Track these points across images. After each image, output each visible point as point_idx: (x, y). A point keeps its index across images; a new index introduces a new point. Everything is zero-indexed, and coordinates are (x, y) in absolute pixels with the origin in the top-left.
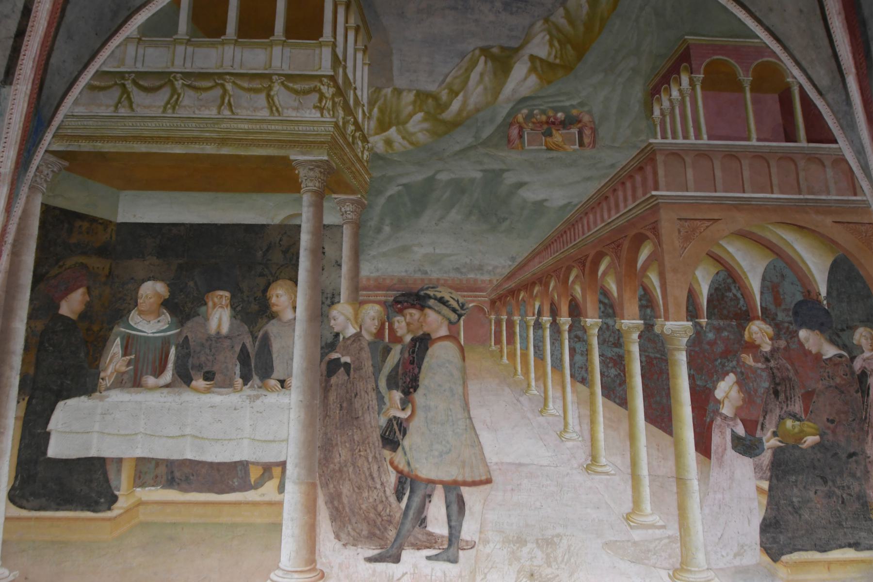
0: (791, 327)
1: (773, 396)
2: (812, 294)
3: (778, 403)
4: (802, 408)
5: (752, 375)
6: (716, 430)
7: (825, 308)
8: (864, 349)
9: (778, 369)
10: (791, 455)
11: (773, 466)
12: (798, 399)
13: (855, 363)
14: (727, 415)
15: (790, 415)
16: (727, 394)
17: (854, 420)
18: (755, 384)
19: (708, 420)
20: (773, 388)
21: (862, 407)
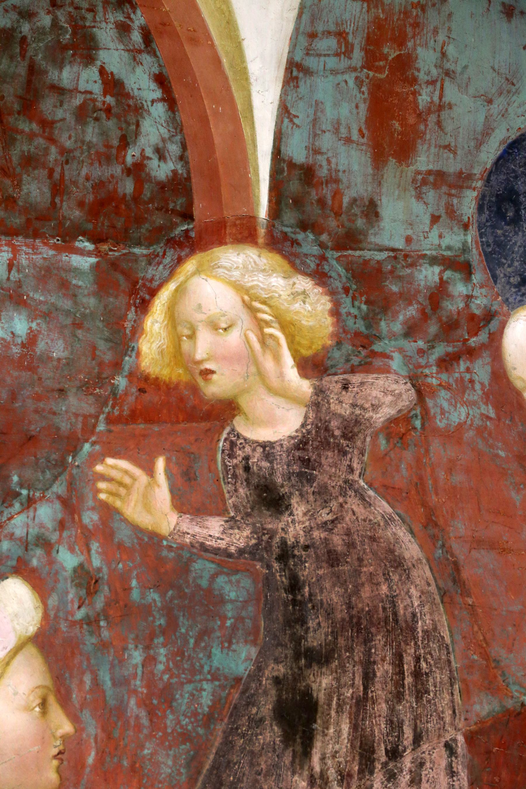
5: (154, 596)
20: (277, 681)
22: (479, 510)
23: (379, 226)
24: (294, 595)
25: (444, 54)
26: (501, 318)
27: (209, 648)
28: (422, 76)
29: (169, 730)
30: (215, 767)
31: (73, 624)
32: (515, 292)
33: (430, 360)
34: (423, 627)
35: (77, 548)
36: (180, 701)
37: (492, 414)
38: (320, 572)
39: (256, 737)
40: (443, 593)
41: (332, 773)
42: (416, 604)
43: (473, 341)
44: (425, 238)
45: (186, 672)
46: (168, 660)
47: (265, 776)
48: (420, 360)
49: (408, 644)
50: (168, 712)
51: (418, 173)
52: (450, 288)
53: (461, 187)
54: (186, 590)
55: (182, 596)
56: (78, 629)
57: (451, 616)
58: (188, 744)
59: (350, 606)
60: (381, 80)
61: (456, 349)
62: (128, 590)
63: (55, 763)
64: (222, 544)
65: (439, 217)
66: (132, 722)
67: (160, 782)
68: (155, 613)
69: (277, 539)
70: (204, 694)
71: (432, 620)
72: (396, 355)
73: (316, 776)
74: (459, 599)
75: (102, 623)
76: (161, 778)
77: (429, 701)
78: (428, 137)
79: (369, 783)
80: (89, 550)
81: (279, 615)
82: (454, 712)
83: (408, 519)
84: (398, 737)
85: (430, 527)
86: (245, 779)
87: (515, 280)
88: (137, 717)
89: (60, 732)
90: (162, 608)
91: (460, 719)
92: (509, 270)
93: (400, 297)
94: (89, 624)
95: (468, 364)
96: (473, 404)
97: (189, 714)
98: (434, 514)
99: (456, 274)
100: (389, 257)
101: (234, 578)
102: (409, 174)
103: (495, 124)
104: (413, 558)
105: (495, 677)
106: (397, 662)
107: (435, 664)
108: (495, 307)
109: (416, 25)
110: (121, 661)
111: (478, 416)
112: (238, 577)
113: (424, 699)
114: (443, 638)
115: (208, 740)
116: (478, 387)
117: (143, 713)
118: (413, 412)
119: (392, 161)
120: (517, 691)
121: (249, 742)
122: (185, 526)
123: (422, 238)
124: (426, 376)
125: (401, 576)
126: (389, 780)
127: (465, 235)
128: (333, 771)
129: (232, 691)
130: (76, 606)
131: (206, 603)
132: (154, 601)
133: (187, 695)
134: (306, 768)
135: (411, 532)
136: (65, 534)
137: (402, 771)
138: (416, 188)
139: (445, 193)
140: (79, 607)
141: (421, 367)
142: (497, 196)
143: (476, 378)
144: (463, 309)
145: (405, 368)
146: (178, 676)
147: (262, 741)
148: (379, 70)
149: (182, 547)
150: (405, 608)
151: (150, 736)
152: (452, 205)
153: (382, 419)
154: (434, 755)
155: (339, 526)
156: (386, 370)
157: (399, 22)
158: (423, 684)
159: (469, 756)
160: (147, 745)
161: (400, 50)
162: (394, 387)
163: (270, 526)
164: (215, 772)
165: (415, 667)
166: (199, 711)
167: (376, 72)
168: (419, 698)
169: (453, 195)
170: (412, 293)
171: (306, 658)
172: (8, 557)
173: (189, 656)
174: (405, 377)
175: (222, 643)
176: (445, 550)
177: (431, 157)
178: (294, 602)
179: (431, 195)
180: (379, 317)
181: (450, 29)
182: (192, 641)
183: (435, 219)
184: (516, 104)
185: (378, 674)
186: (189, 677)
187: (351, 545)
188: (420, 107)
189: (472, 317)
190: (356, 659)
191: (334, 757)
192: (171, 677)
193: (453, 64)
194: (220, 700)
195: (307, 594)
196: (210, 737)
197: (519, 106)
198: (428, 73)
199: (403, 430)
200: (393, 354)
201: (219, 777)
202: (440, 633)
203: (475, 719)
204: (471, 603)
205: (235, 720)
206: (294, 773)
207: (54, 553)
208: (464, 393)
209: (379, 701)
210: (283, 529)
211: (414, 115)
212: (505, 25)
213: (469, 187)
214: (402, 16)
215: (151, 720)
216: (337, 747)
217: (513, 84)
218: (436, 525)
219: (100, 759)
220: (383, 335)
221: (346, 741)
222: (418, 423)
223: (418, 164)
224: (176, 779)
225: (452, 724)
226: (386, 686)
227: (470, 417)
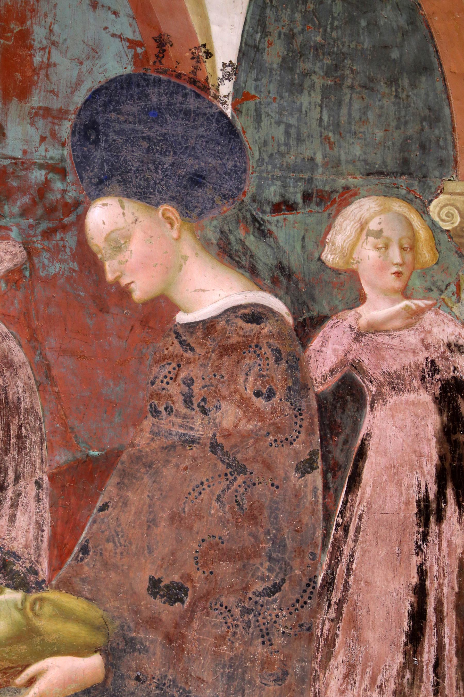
0: (58, 185)
2: (171, 52)
4: (46, 535)
7: (222, 114)
8: (366, 289)
12: (32, 490)
13: (315, 344)
17: (276, 588)
21: (319, 534)
22: (66, 330)
23: (5, 143)
25: (51, 31)
26: (85, 205)
28: (36, 45)
32: (95, 189)
33: (37, 232)
34: (24, 406)
37: (77, 268)
40: (39, 385)
42: (20, 391)
43: (66, 220)
44: (36, 151)
48: (31, 232)
49: (14, 418)
51: (33, 108)
52: (52, 185)
53: (61, 119)
57: (44, 399)
60: (8, 45)
61: (54, 225)
65: (46, 138)
72: (14, 229)
74: (49, 388)
77: (26, 454)
78: (39, 84)
82: (42, 461)
83: (18, 337)
84: (5, 477)
85: (32, 342)
87: (95, 181)
92: (91, 174)
93: (18, 190)
95: (62, 235)
96: (62, 261)
98: (35, 333)
99: (56, 176)
100: (11, 163)
102: (26, 108)
103: (85, 78)
104: (20, 361)
105: (71, 438)
107: (32, 430)
108: (81, 198)
109: (33, 10)
111: (67, 269)
114: (37, 413)
116: (68, 250)
118: (24, 266)
119: (15, 100)
120: (84, 447)
123: (34, 151)
124: (34, 242)
125: (11, 373)
127: (63, 150)
135: (20, 345)
137: (6, 499)
138: (31, 118)
139: (50, 122)
141: (31, 236)
142: (85, 125)
143: (67, 244)
144: (60, 199)
145: (20, 237)
148: (8, 39)
150: (13, 394)
152: (55, 130)
153: (3, 270)
156: (7, 238)
157: (21, 8)
158: (22, 443)
159: (51, 489)
161: (22, 27)
162: (12, 249)
165: (18, 432)
167: (5, 40)
168: (19, 452)
169: (55, 124)
170: (27, 187)
174: (19, 243)
176: (41, 356)
177: (41, 98)
179: (40, 123)
180: (4, 203)
181: (55, 15)
183: (43, 139)
184: (98, 65)
188: (35, 65)
189: (66, 205)
193: (57, 38)
197: (100, 67)
198: (41, 42)
199: (17, 278)
200: (12, 227)
203: (56, 465)
208: (58, 254)
211: (30, 70)
212: (92, 14)
213: (66, 119)
214: (23, 4)
217: (96, 52)
218: (36, 340)
220: (6, 215)
222: (27, 273)
223: (33, 102)
225: (40, 469)
227: (62, 270)
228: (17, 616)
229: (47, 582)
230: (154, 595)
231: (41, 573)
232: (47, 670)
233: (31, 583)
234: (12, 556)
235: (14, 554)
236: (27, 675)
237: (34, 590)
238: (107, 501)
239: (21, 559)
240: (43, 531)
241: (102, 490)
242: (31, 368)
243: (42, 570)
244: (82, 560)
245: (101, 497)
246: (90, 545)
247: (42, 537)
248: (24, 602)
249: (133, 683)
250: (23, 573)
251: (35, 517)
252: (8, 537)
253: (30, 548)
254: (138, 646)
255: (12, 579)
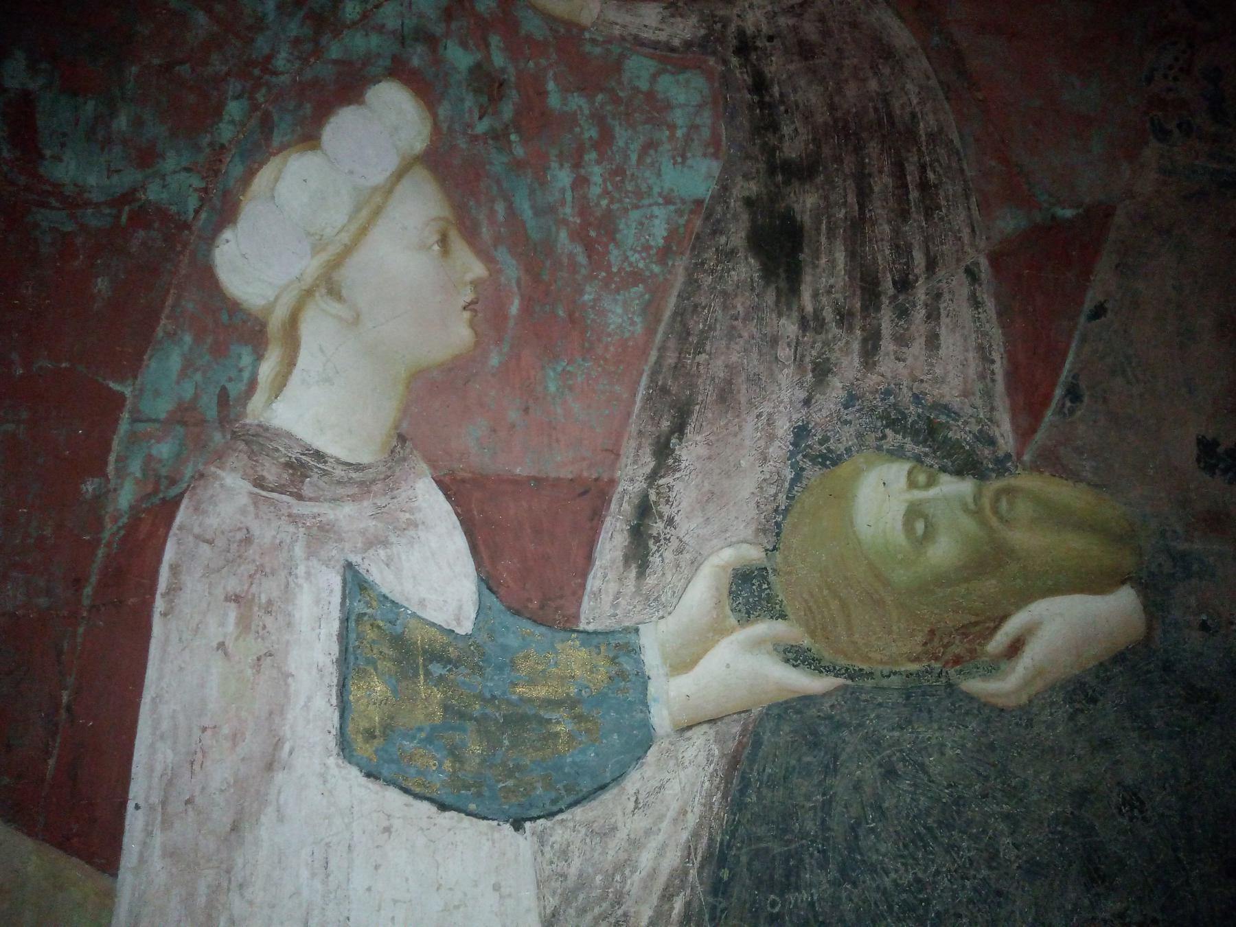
1: (746, 269)
3: (789, 327)
4: (998, 368)
5: (577, 102)
6: (193, 585)
9: (806, 51)
10: (890, 773)
11: (718, 888)
14: (322, 443)
15: (895, 421)
16: (336, 263)
18: (596, 173)
19: (126, 497)
20: (749, 202)
24: (762, 96)
27: (657, 165)
29: (615, 270)
30: (679, 313)
31: (475, 138)
35: (471, 42)
36: (625, 232)
38: (792, 67)
39: (728, 272)
41: (828, 314)
42: (915, 101)
45: (630, 195)
46: (605, 181)
47: (744, 320)
50: (611, 246)
54: (621, 94)
55: (616, 100)
56: (482, 144)
58: (640, 285)
59: (832, 107)
62: (543, 94)
63: (467, 315)
64: (662, 37)
66: (565, 261)
67: (609, 335)
68: (582, 122)
69: (732, 28)
70: (657, 222)
71: (937, 121)
73: (809, 318)
75: (513, 137)
76: (609, 330)
77: (941, 219)
79: (875, 322)
80: (487, 45)
81: (743, 120)
82: (973, 230)
84: (907, 264)
86: (718, 326)
88: (571, 256)
89: (469, 277)
90: (592, 116)
91: (981, 239)
94: (496, 138)
97: (639, 249)
101: (681, 77)
106: (898, 174)
110: (543, 183)
112: (687, 75)
113: (935, 216)
114: (952, 141)
115: (666, 279)
117: (578, 250)
121: (720, 279)
122: (612, 15)
126: (900, 317)
128: (830, 310)
129: (692, 216)
130: (476, 115)
131: (648, 109)
132: (580, 107)
133: (634, 225)
134: (795, 307)
136: (454, 26)
137: (915, 306)
140: (480, 118)
146: (620, 201)
147: (736, 278)
149: (609, 41)
151: (591, 278)
154: (954, 283)
155: (810, 10)
160: (588, 288)
163: (721, 13)
164: (679, 319)
165: (920, 178)
166: (652, 243)
171: (783, 174)
172: (379, 55)
173: (633, 175)
175: (674, 158)
178: (762, 105)
182: (634, 157)
185: (876, 189)
186: (635, 201)
187: (826, 34)
190: (847, 171)
191: (829, 292)
192: (612, 201)
194: (677, 229)
195: (777, 95)
196: (669, 277)
201: (684, 324)
202: (947, 136)
204: (981, 98)
205: (699, 253)
206: (780, 315)
207: (441, 51)
209: (880, 221)
210: (739, 16)
215: (589, 257)
216: (832, 281)
219: (526, 309)
221: (843, 272)
224: (630, 331)
225: (972, 245)
226: (887, 203)
228: (969, 525)
229: (1014, 458)
230: (1210, 469)
231: (1001, 441)
232: (1041, 623)
233: (985, 462)
234: (943, 413)
235: (946, 409)
236: (1006, 634)
237: (994, 475)
238: (1101, 298)
239: (959, 416)
240: (993, 362)
241: (1088, 280)
242: (928, 58)
243: (1002, 435)
244: (1072, 411)
245: (1090, 294)
246: (1083, 385)
247: (993, 373)
248: (977, 497)
249: (1196, 635)
250: (968, 443)
251: (974, 336)
252: (929, 377)
253: (974, 394)
254: (1195, 567)
255: (949, 456)
